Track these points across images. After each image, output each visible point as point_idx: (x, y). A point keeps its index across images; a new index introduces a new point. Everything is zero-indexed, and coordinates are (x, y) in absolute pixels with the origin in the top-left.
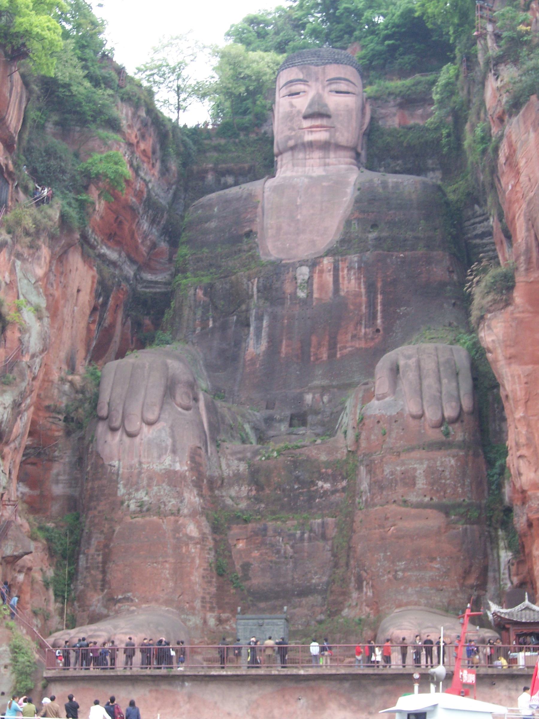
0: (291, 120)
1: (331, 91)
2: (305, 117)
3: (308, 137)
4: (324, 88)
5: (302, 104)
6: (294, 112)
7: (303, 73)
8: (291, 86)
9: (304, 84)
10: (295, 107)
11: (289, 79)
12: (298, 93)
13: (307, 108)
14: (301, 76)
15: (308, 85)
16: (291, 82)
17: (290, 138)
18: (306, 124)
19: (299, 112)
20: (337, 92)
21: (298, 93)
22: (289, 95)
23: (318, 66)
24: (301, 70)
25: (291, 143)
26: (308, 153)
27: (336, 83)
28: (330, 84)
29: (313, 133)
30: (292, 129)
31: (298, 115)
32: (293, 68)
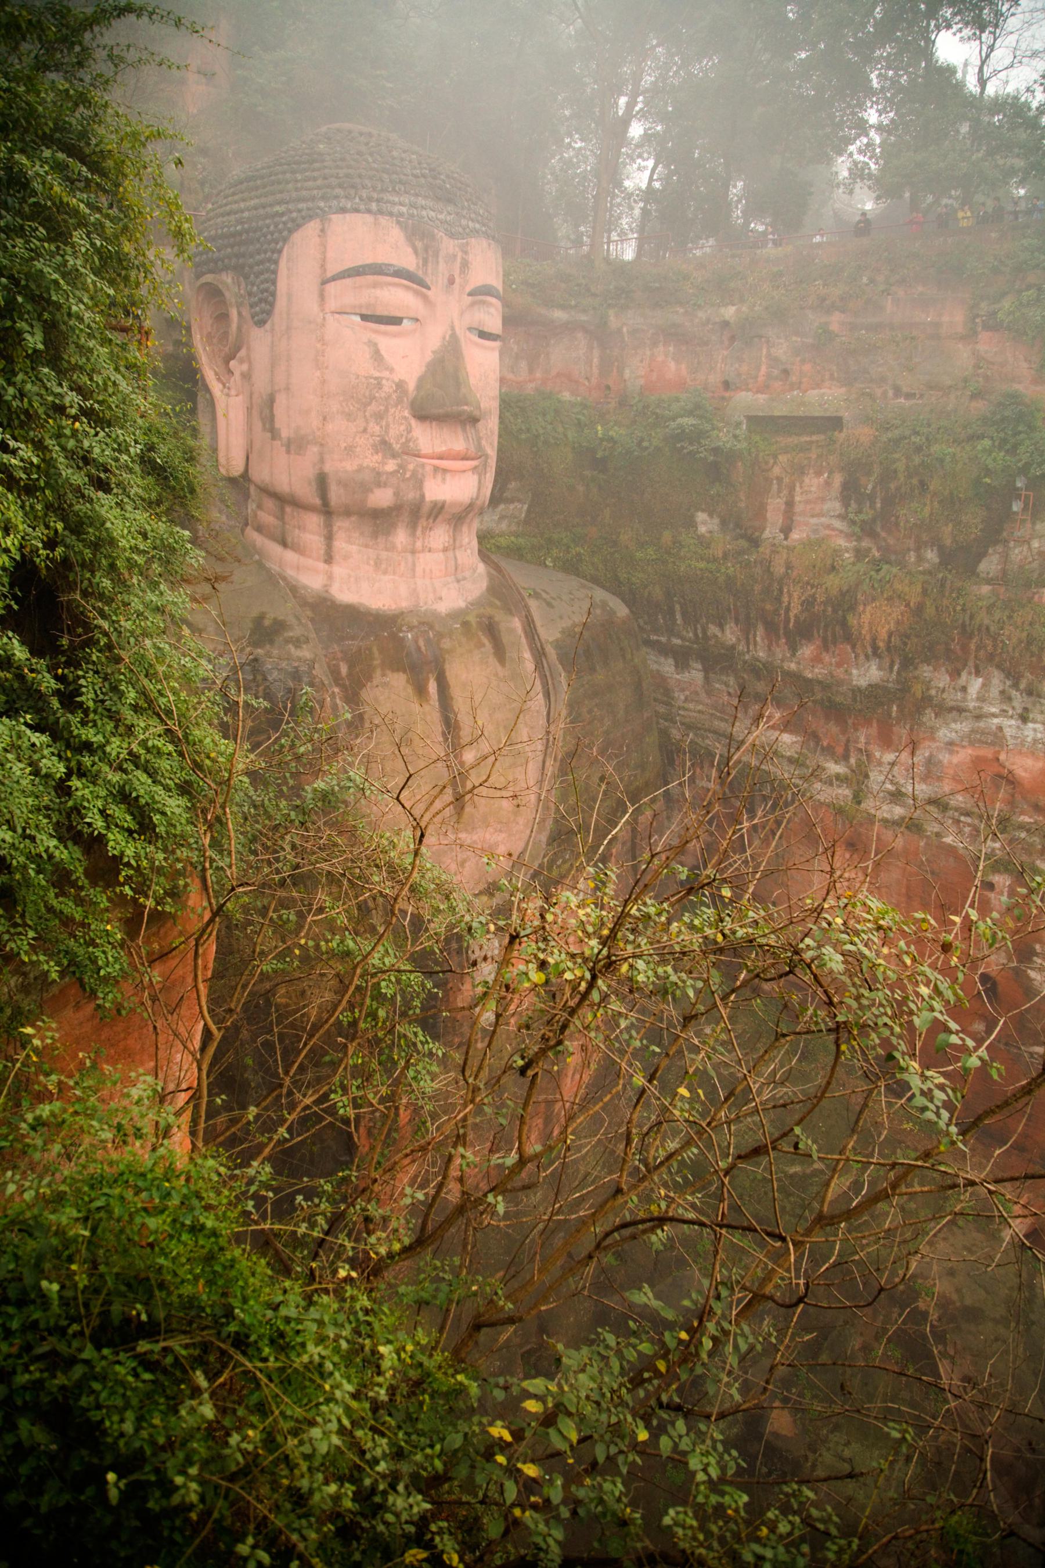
0: (379, 417)
1: (470, 329)
2: (423, 416)
3: (436, 491)
4: (462, 314)
5: (406, 358)
6: (388, 387)
7: (416, 252)
8: (375, 286)
9: (417, 293)
10: (392, 370)
11: (368, 259)
12: (396, 321)
13: (421, 380)
14: (408, 260)
15: (425, 298)
16: (377, 270)
17: (379, 480)
18: (428, 439)
19: (400, 386)
20: (483, 335)
21: (396, 321)
22: (364, 318)
23: (452, 236)
24: (410, 238)
25: (382, 498)
26: (419, 532)
27: (484, 302)
28: (473, 304)
29: (448, 476)
30: (384, 446)
31: (399, 401)
32: (383, 220)
